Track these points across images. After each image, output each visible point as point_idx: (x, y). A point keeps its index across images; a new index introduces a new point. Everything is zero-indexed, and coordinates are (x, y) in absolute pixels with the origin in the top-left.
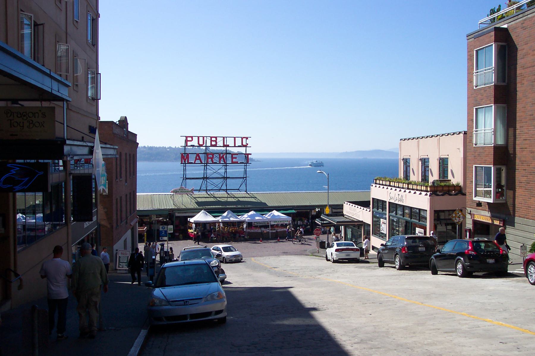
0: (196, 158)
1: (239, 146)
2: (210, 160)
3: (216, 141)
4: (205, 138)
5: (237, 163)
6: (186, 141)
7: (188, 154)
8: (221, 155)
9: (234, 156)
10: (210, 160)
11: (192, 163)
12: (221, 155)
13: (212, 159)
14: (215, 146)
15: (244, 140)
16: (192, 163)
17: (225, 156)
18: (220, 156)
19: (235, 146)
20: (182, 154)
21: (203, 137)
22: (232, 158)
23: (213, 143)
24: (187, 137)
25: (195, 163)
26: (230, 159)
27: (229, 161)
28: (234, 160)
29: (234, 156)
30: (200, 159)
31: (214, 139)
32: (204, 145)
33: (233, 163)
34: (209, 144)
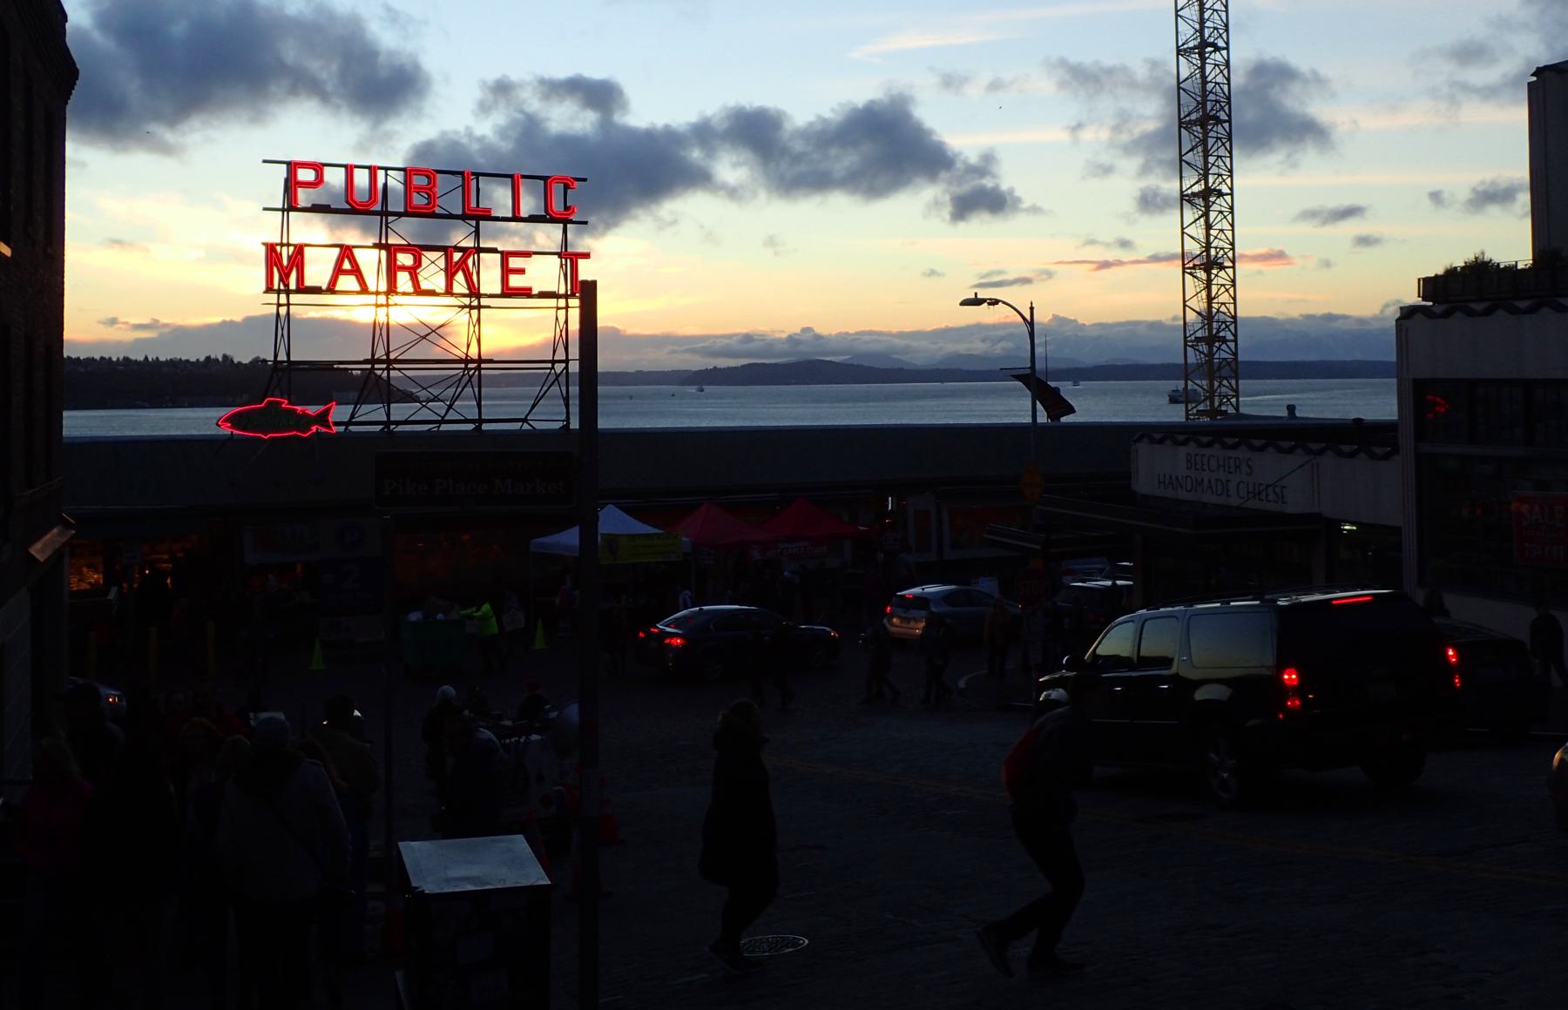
0: (339, 262)
1: (533, 219)
2: (403, 280)
3: (429, 191)
4: (381, 173)
5: (526, 293)
6: (291, 185)
7: (299, 250)
8: (457, 256)
9: (514, 263)
10: (403, 280)
11: (316, 290)
12: (457, 256)
13: (413, 271)
14: (427, 213)
15: (558, 189)
16: (316, 290)
17: (470, 262)
18: (449, 259)
19: (516, 218)
20: (271, 249)
21: (373, 170)
22: (506, 271)
23: (419, 200)
24: (292, 167)
25: (331, 289)
26: (497, 273)
27: (490, 277)
28: (515, 281)
29: (514, 263)
30: (356, 271)
31: (420, 181)
32: (377, 207)
33: (508, 292)
34: (396, 205)
